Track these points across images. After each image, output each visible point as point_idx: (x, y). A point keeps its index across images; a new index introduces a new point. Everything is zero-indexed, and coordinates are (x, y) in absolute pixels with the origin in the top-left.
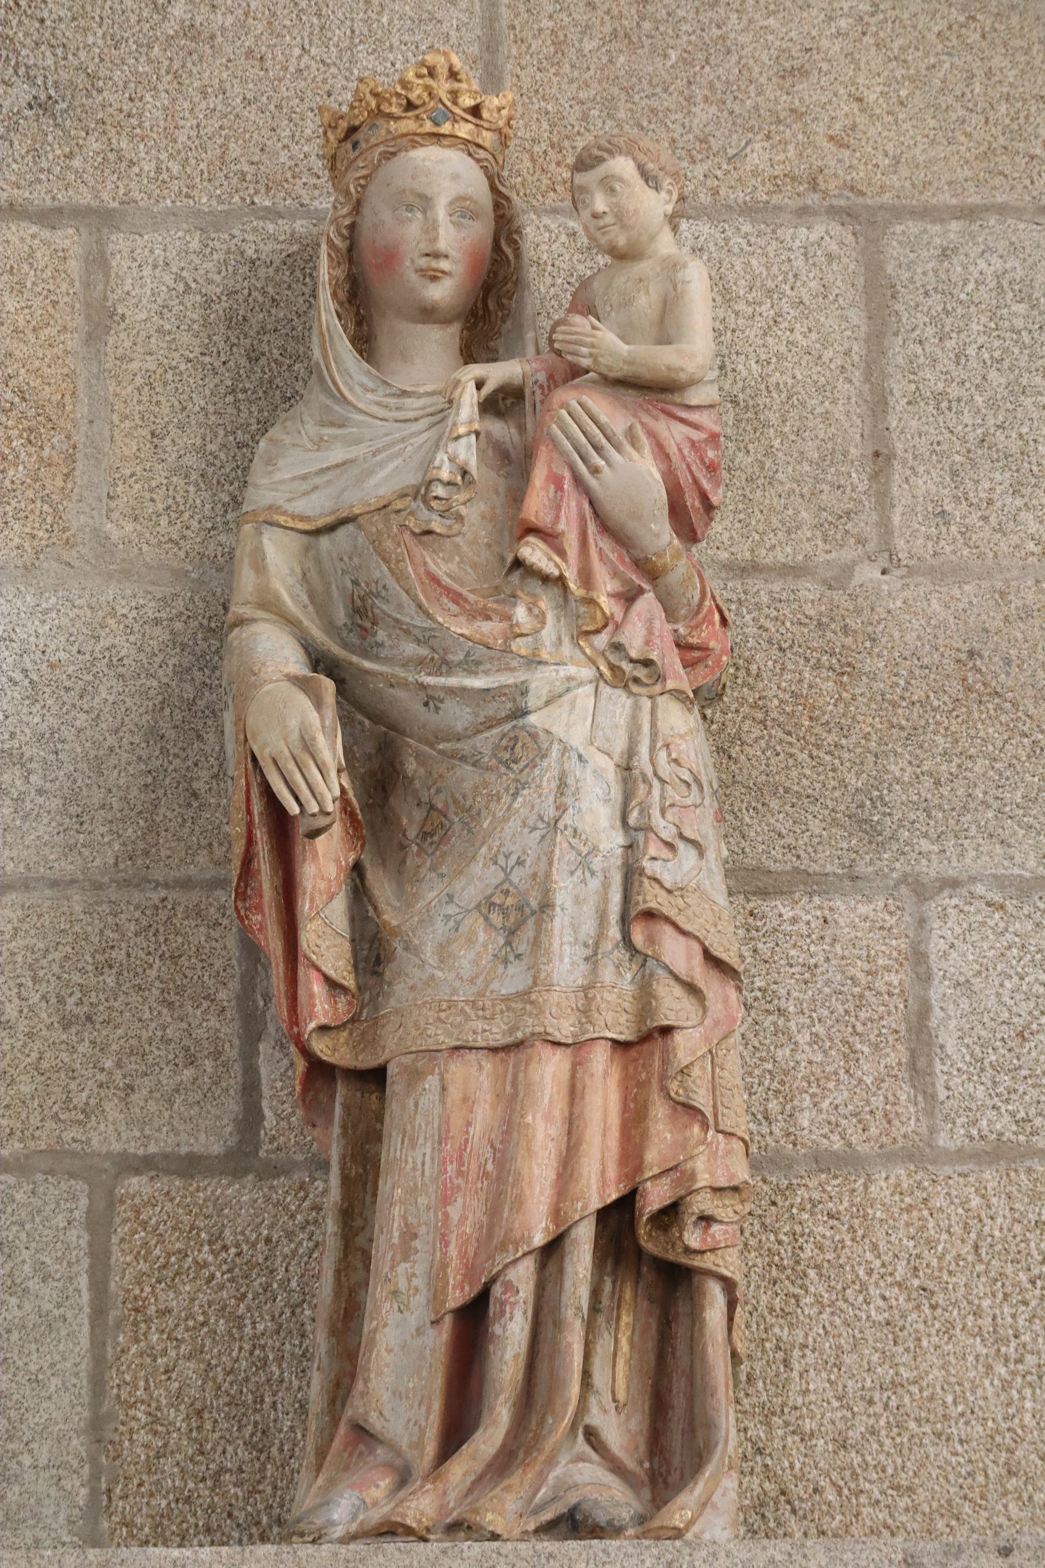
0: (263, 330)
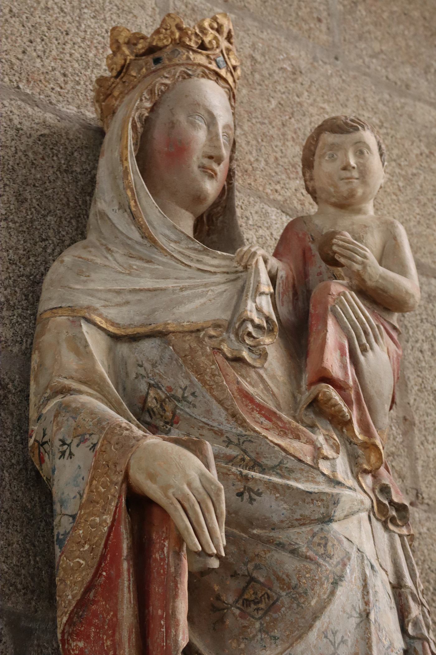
0: (25, 182)
